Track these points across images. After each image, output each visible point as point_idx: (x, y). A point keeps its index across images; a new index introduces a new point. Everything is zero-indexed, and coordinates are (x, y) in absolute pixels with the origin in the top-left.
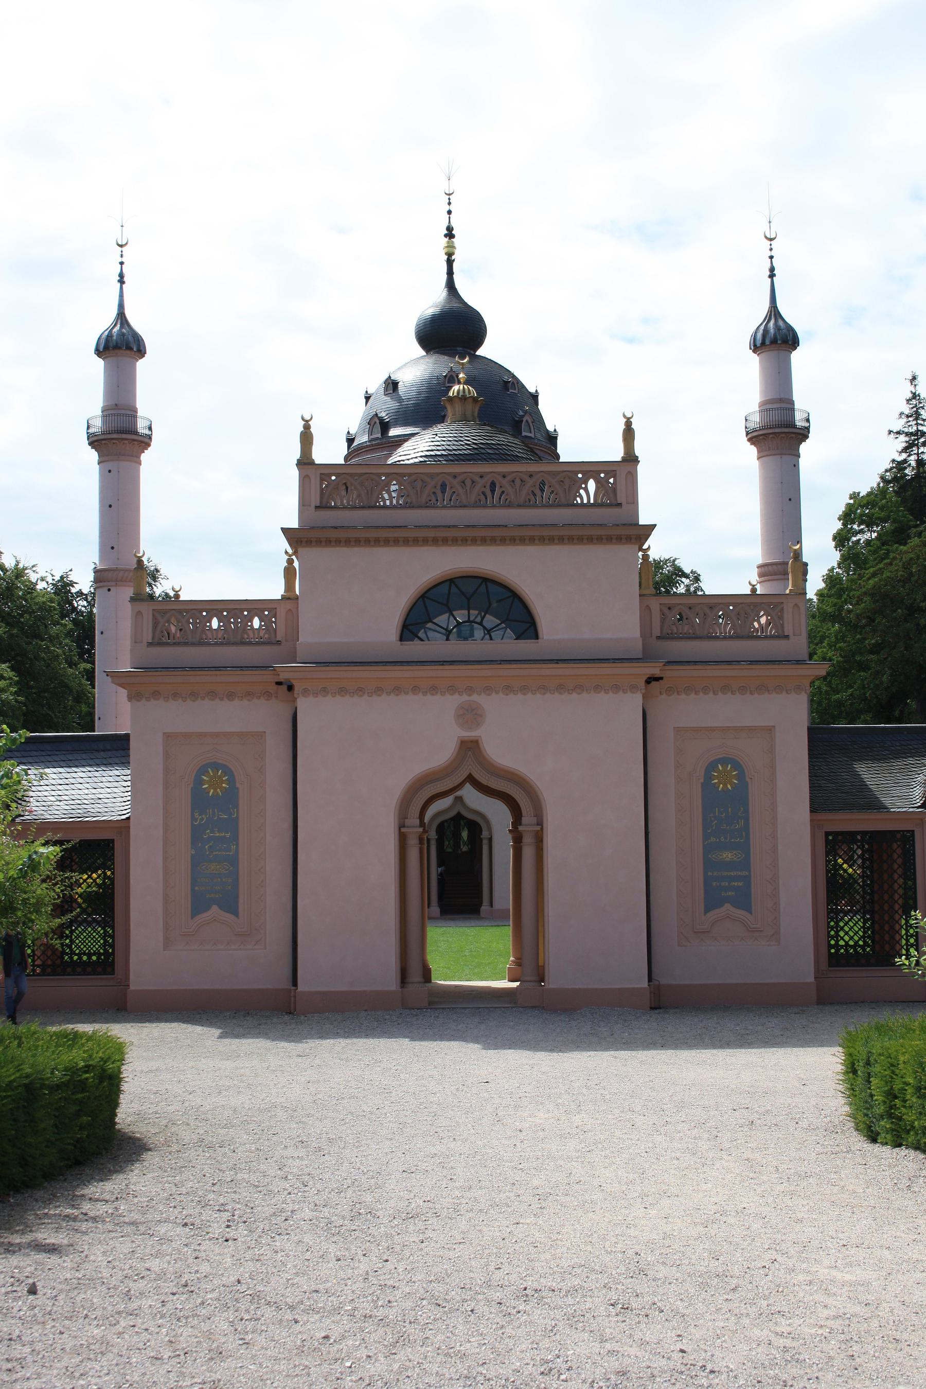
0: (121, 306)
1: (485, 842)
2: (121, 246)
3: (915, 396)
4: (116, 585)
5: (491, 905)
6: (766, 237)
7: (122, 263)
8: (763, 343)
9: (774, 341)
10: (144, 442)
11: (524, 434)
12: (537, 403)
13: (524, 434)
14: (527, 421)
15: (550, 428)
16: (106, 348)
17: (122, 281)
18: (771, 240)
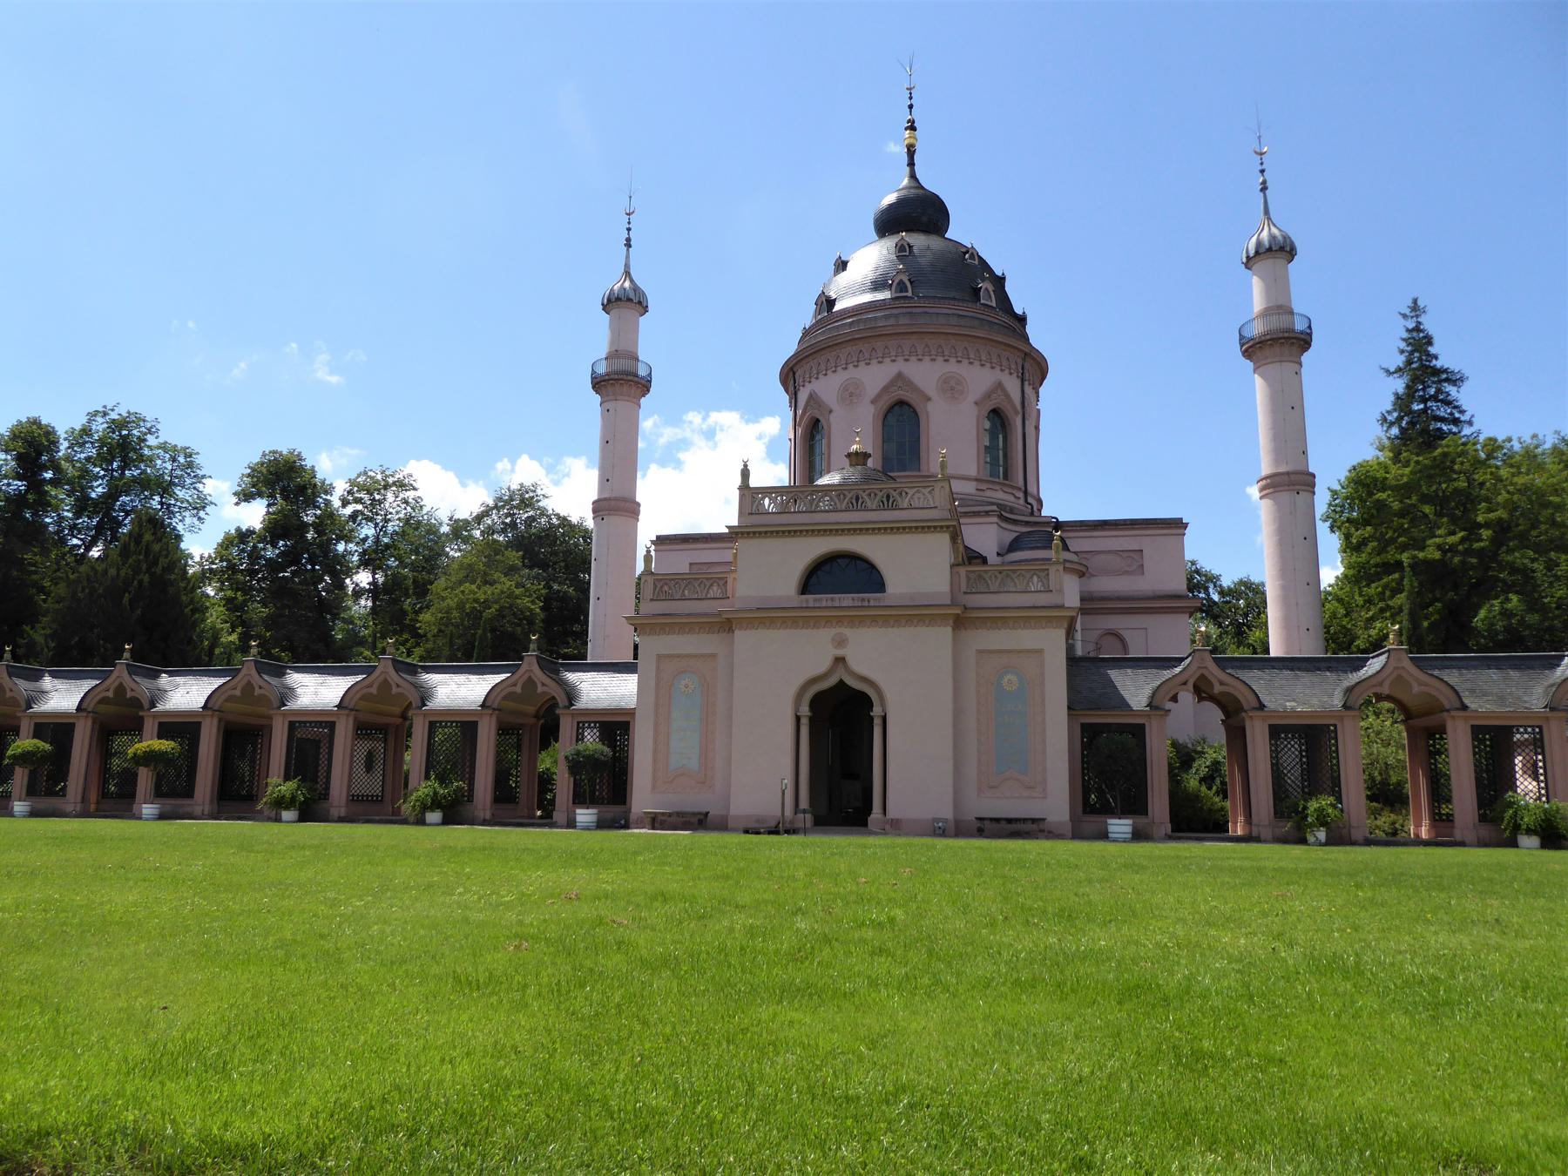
0: (627, 266)
1: (877, 722)
2: (629, 214)
3: (1417, 329)
4: (609, 515)
5: (885, 814)
6: (1256, 152)
7: (629, 229)
8: (1257, 253)
9: (1270, 249)
10: (644, 386)
11: (982, 301)
12: (1003, 287)
13: (982, 301)
14: (986, 289)
15: (1018, 310)
16: (609, 300)
17: (628, 244)
18: (1262, 154)
